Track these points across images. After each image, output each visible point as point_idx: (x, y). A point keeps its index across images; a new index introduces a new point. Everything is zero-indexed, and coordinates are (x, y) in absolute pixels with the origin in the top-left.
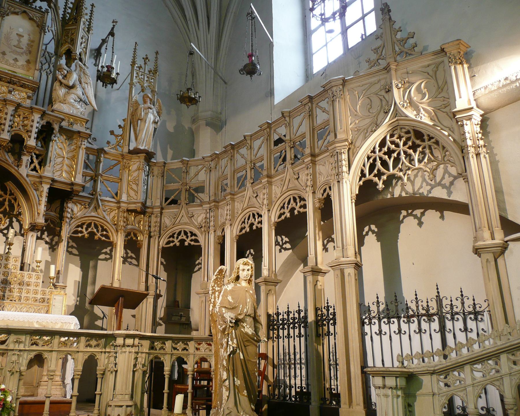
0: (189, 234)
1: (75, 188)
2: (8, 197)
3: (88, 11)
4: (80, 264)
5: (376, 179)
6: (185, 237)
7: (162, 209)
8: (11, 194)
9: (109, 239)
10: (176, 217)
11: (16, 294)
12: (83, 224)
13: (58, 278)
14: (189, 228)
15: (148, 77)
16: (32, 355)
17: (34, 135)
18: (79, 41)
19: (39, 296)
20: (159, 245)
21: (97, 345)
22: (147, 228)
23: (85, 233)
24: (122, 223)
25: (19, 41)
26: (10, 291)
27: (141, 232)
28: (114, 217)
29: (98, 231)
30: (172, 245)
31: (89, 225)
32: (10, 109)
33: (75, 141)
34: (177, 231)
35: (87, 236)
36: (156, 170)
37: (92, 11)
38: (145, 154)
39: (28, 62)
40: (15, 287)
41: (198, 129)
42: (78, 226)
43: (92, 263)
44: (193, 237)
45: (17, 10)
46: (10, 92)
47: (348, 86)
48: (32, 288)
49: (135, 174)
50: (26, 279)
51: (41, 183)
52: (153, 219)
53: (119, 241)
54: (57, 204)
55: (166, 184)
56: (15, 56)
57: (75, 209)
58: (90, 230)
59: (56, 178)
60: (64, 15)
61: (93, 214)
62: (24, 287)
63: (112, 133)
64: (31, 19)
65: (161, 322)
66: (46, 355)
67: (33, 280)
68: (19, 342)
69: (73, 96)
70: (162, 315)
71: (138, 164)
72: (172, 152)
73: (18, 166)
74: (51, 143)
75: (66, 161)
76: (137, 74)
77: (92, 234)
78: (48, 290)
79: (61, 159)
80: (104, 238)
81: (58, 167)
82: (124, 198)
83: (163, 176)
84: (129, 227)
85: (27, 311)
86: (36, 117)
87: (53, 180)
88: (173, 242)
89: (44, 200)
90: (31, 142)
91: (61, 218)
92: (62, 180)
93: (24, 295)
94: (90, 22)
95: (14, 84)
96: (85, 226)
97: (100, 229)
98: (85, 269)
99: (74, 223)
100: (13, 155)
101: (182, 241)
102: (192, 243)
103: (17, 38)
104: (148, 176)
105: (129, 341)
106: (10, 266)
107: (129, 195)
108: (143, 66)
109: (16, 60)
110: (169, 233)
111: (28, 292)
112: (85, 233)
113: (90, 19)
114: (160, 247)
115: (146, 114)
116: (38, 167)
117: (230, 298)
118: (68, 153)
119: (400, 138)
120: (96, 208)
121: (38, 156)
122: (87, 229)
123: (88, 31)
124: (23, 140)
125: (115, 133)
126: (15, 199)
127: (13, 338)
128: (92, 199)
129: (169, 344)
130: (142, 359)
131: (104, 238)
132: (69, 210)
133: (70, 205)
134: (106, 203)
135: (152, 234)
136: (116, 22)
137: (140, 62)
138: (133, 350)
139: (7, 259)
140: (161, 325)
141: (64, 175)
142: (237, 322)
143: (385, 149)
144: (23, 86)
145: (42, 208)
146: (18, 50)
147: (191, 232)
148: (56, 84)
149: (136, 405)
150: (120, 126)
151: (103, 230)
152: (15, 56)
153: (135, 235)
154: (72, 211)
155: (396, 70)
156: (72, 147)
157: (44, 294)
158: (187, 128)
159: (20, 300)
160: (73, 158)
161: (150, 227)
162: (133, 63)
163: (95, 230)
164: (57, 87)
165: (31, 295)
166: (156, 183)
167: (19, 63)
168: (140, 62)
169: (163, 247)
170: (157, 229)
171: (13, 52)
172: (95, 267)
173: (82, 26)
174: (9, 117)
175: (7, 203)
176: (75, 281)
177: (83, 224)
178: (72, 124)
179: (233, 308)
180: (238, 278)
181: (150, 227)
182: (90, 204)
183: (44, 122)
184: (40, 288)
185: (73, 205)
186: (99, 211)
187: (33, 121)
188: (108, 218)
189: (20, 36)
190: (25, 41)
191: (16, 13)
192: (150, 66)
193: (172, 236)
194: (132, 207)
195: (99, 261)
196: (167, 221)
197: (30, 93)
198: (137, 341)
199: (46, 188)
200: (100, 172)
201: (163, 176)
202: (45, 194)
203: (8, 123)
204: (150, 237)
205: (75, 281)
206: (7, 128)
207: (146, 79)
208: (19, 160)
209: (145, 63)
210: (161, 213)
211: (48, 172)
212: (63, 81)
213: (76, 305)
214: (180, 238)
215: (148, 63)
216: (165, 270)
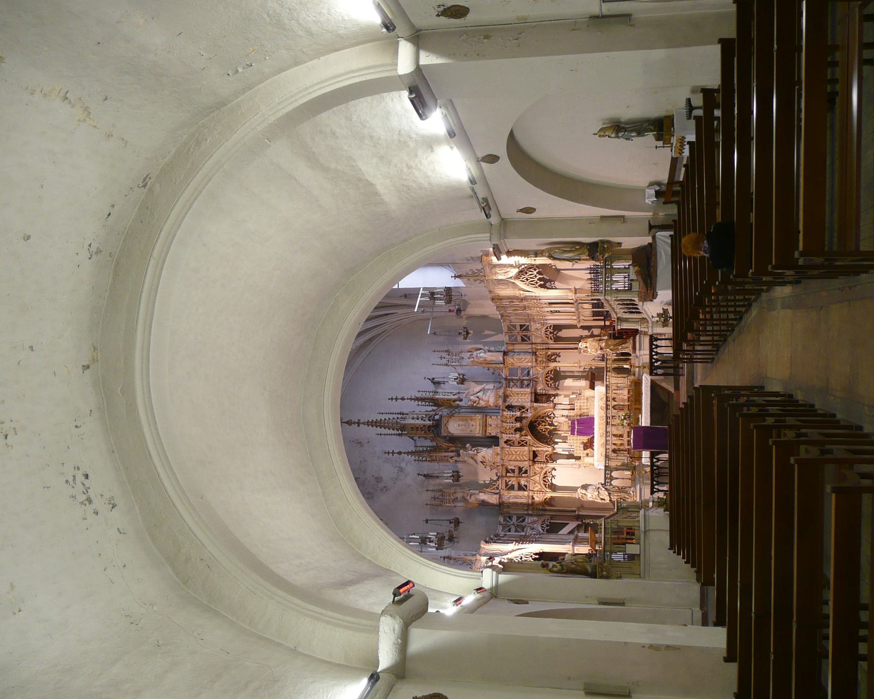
0: (547, 330)
1: (533, 391)
2: (539, 419)
3: (424, 394)
4: (564, 380)
5: (538, 284)
6: (549, 332)
7: (532, 344)
8: (537, 418)
9: (552, 370)
10: (537, 337)
11: (585, 411)
12: (546, 383)
13: (575, 393)
14: (544, 330)
15: (453, 356)
16: (613, 409)
17: (514, 413)
18: (446, 397)
19: (585, 401)
20: (553, 344)
21: (609, 390)
22: (544, 351)
23: (551, 382)
24: (544, 365)
25: (462, 425)
26: (584, 413)
27: (547, 353)
28: (540, 368)
29: (549, 376)
30: (552, 338)
31: (547, 381)
32: (504, 424)
33: (508, 394)
34: (545, 335)
35: (552, 381)
36: (510, 348)
37: (423, 392)
38: (505, 357)
39: (472, 420)
40: (583, 411)
41: (466, 315)
42: (548, 386)
43: (562, 374)
44: (549, 328)
45: (446, 428)
46: (491, 426)
47: (492, 290)
48: (582, 405)
49: (515, 360)
50: (578, 407)
51: (533, 407)
52: (539, 347)
53: (552, 365)
54: (538, 397)
55: (517, 341)
56: (471, 426)
57: (539, 388)
58: (549, 380)
59: (529, 400)
60: (432, 406)
61: (541, 379)
62: (582, 407)
63: (493, 374)
64: (448, 422)
65: (591, 331)
66: (613, 405)
67: (578, 404)
68: (609, 413)
69: (484, 397)
70: (587, 331)
71: (510, 359)
72: (486, 331)
73: (527, 417)
74: (513, 405)
75: (520, 395)
76: (453, 362)
77: (551, 379)
78: (582, 398)
79: (519, 399)
80: (553, 373)
81: (524, 400)
82: (530, 364)
83: (513, 344)
84: (544, 360)
85: (594, 406)
86: (505, 413)
87: (531, 401)
88: (551, 337)
89: (541, 405)
90: (518, 414)
91: (546, 395)
92: (529, 397)
93: (585, 407)
94: (430, 392)
95: (486, 424)
96: (548, 383)
97: (548, 375)
98: (566, 377)
99: (548, 388)
100: (522, 420)
101: (551, 333)
102: (552, 328)
103: (460, 426)
104: (514, 352)
105: (608, 380)
106: (573, 415)
107: (528, 362)
108: (447, 359)
109: (473, 425)
110: (546, 339)
111: (584, 406)
112: (551, 382)
113: (428, 392)
114: (554, 343)
115: (481, 357)
116: (526, 409)
117: (593, 350)
118: (515, 397)
119: (521, 277)
120: (538, 378)
121: (520, 410)
122: (549, 382)
123: (437, 392)
124: (517, 417)
125: (493, 371)
126: (540, 416)
127: (608, 415)
128: (533, 381)
129: (608, 366)
130: (613, 375)
131: (553, 373)
132: (541, 391)
133: (539, 391)
134: (534, 373)
135: (547, 347)
136: (425, 378)
137: (444, 361)
138: (610, 378)
139: (570, 416)
140: (592, 331)
141: (527, 396)
142: (601, 349)
143: (526, 281)
144: (486, 420)
145: (545, 405)
146: (467, 425)
147: (546, 329)
148: (478, 406)
149: (627, 376)
150: (488, 370)
151: (548, 373)
152: (471, 426)
153: (548, 356)
154: (540, 390)
155: (488, 276)
156: (512, 394)
157: (584, 399)
158: (467, 322)
159: (587, 409)
160: (518, 394)
161: (543, 349)
162: (447, 365)
163: (549, 377)
164: (481, 405)
165: (585, 405)
166: (517, 347)
167: (474, 424)
168: (444, 361)
169: (554, 342)
170: (544, 345)
171: (469, 426)
172: (564, 372)
173: (437, 397)
174: (509, 424)
175: (542, 420)
176: (573, 381)
177: (546, 383)
178: (500, 396)
179: (597, 349)
180: (586, 347)
181: (543, 349)
182: (536, 382)
183: (506, 410)
184: (582, 401)
185: (537, 389)
186: (539, 376)
187: (507, 414)
188: (541, 372)
189: (459, 425)
190: (461, 423)
191: (447, 428)
192: (445, 355)
193: (548, 338)
194: (534, 360)
195: (561, 370)
196: (539, 341)
197: (488, 417)
198: (608, 377)
199: (535, 404)
200: (518, 378)
201: (513, 344)
202: (539, 405)
203: (511, 424)
204: (549, 349)
205: (573, 381)
206: (514, 425)
207: (454, 357)
208: (524, 417)
209: (444, 358)
210: (535, 344)
211: (528, 405)
212: (477, 403)
213: (585, 380)
214: (549, 334)
215: (443, 356)
216: (561, 331)
